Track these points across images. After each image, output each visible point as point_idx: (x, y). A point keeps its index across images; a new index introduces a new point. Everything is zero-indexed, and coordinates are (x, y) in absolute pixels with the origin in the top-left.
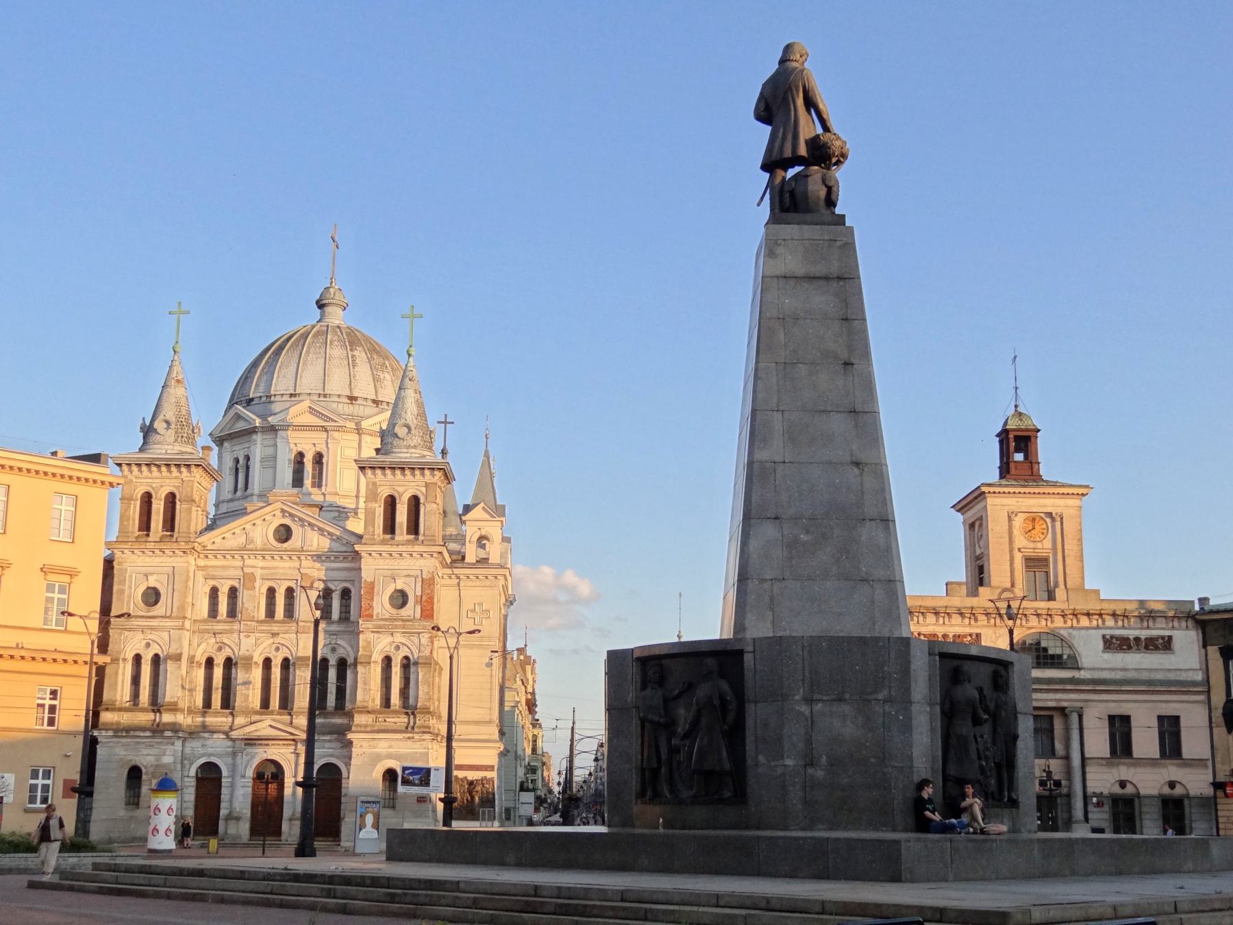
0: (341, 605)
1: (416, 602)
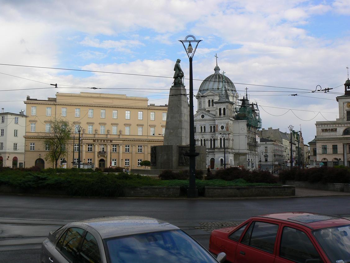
0: (214, 129)
1: (225, 128)
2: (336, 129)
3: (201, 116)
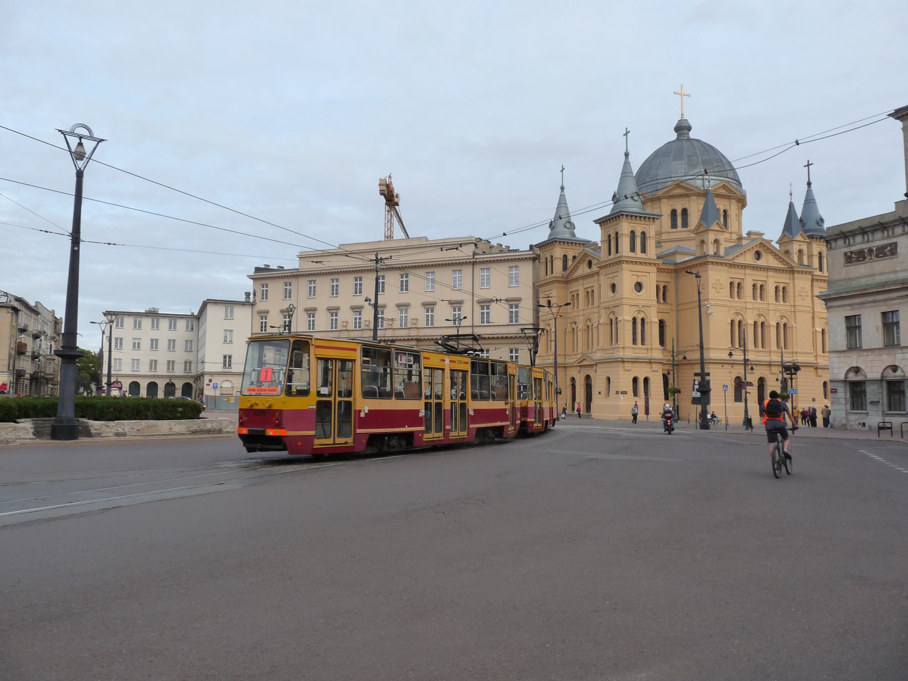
2: (896, 244)
3: (586, 265)
